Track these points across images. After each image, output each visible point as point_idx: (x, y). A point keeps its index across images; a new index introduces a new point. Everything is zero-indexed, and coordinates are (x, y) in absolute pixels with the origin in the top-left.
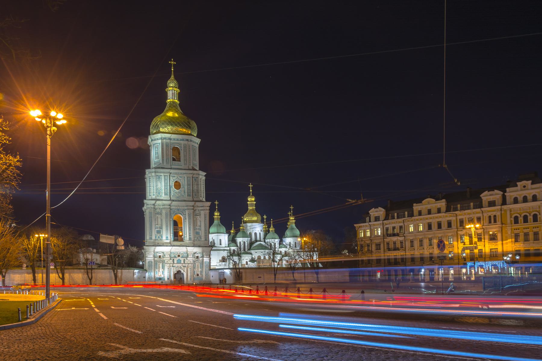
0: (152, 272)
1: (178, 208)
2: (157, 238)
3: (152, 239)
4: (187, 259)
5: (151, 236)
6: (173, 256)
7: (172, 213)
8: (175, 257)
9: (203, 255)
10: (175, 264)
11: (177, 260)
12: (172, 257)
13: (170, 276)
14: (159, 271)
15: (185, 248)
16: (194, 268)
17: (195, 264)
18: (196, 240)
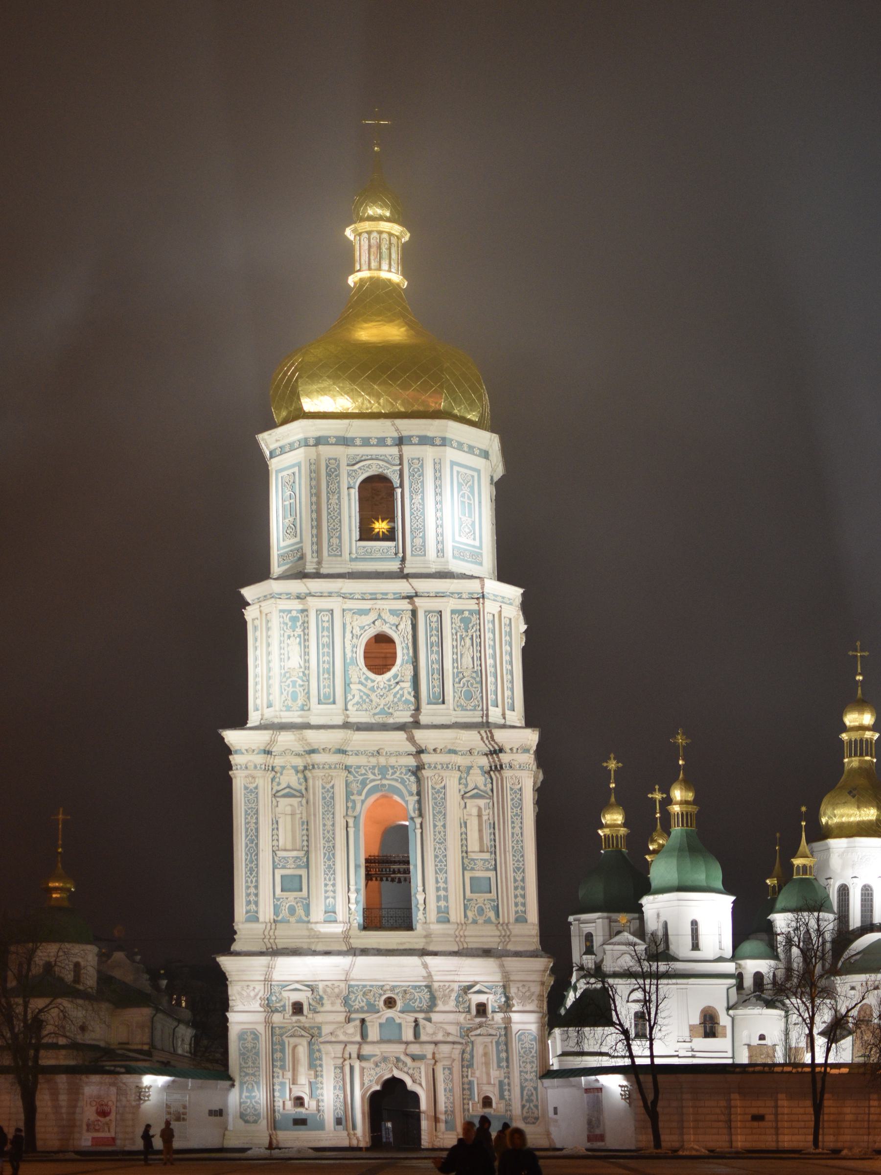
0: (258, 1083)
1: (382, 761)
2: (284, 913)
3: (257, 920)
4: (429, 1020)
5: (253, 907)
6: (359, 1002)
7: (354, 787)
8: (372, 1009)
9: (508, 999)
10: (373, 1043)
11: (381, 1025)
12: (357, 1011)
13: (347, 1106)
14: (294, 1082)
15: (414, 960)
16: (467, 1064)
17: (472, 1043)
18: (475, 922)
